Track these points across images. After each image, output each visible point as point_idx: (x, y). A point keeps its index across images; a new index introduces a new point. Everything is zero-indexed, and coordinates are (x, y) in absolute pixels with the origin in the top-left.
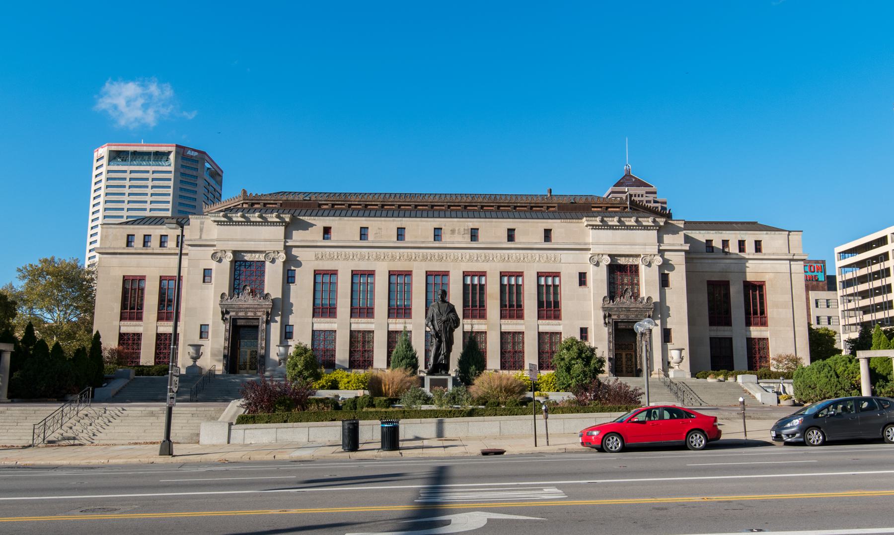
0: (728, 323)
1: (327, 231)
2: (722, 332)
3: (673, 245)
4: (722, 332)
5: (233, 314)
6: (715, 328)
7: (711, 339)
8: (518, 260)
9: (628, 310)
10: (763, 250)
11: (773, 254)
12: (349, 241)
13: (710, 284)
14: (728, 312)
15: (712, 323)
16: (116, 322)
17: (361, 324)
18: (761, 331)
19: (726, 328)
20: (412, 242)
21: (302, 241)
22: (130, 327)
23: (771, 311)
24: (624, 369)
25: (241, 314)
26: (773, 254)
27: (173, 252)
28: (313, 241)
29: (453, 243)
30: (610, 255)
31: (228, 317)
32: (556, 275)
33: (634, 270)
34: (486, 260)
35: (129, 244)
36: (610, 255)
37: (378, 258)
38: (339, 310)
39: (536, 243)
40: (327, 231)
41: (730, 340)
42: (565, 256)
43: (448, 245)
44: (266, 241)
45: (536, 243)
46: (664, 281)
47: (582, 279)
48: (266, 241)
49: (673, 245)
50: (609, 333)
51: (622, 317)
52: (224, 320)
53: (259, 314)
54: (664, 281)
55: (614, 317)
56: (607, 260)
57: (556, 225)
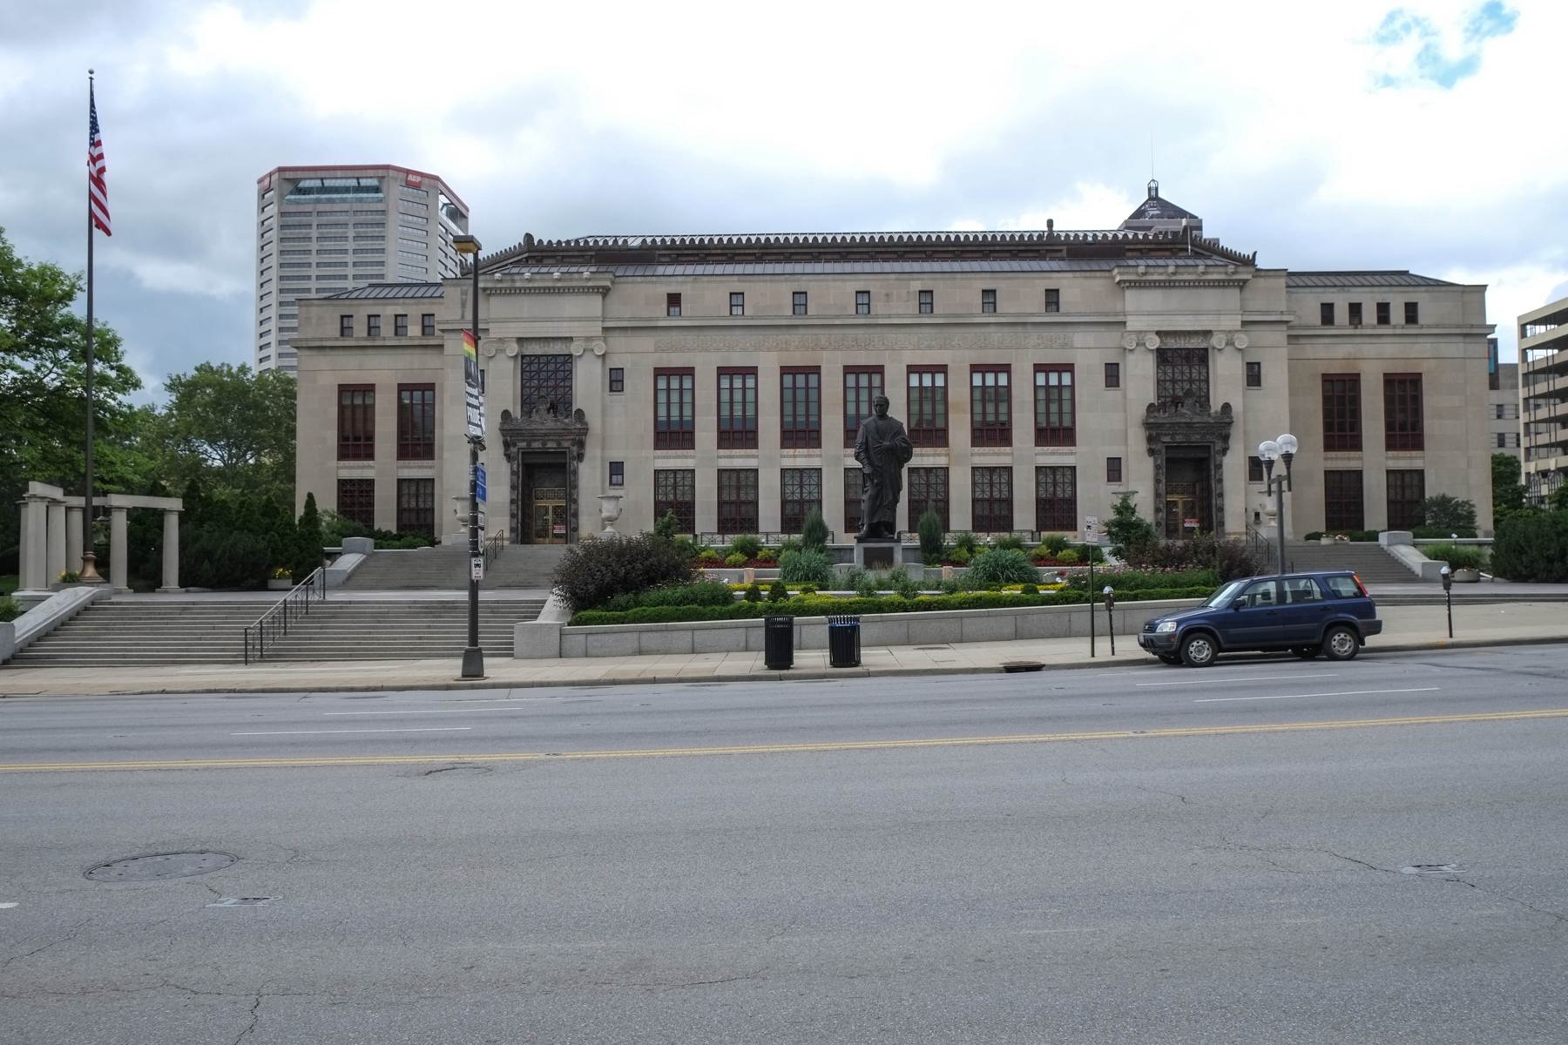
0: (1357, 446)
1: (674, 300)
2: (1343, 461)
3: (1267, 313)
5: (524, 444)
6: (1333, 454)
7: (1326, 473)
9: (1189, 425)
10: (1422, 319)
11: (1437, 326)
12: (711, 318)
13: (1328, 379)
14: (1356, 425)
15: (1329, 446)
16: (333, 462)
17: (738, 459)
20: (818, 317)
21: (629, 320)
22: (355, 470)
23: (1430, 425)
25: (536, 445)
27: (416, 342)
28: (650, 319)
29: (889, 316)
30: (1158, 333)
31: (514, 450)
32: (1069, 368)
35: (345, 330)
36: (1158, 333)
37: (757, 349)
38: (699, 436)
39: (1032, 315)
40: (674, 300)
41: (1359, 474)
42: (1080, 338)
43: (880, 321)
44: (572, 320)
45: (1032, 315)
46: (1254, 376)
47: (1112, 375)
48: (572, 320)
49: (1267, 313)
50: (1157, 467)
51: (1179, 438)
52: (508, 457)
53: (566, 444)
54: (1254, 376)
55: (1167, 439)
57: (1065, 282)
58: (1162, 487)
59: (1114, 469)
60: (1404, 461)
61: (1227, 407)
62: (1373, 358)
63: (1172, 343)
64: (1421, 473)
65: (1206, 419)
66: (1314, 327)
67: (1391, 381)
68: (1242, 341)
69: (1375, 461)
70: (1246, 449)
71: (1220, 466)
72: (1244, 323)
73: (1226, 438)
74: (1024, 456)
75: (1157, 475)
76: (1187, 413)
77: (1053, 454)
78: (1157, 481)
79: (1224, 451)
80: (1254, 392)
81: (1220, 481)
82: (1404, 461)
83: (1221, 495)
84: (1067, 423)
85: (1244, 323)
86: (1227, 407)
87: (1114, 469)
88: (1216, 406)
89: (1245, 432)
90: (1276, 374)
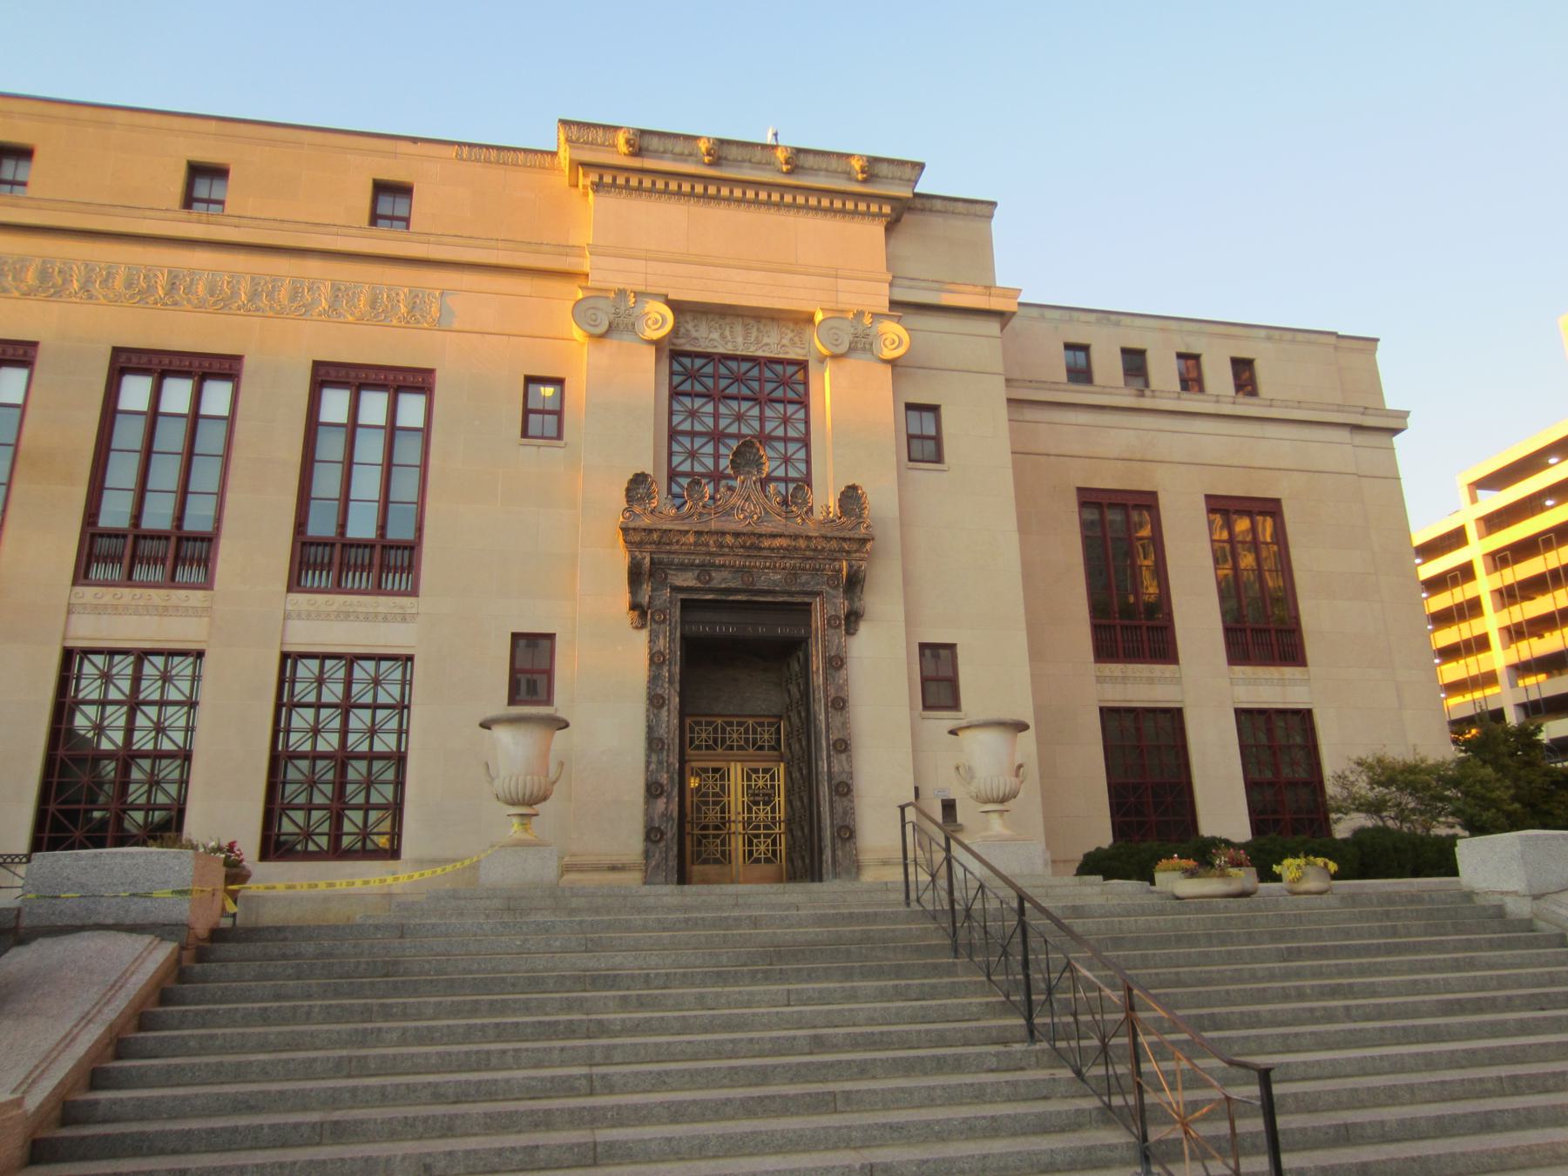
2: (1141, 686)
4: (1141, 686)
6: (1115, 669)
8: (221, 301)
11: (1300, 404)
13: (1090, 499)
18: (1282, 682)
19: (1158, 669)
23: (1314, 614)
24: (738, 845)
26: (1300, 404)
32: (418, 381)
33: (786, 383)
34: (50, 285)
41: (1175, 716)
46: (924, 440)
50: (656, 660)
51: (720, 579)
54: (924, 440)
55: (687, 580)
56: (658, 321)
58: (669, 719)
59: (531, 668)
60: (1271, 688)
61: (851, 497)
62: (1183, 462)
63: (712, 339)
64: (1305, 716)
65: (796, 526)
66: (1054, 385)
67: (1221, 507)
68: (894, 337)
69: (1208, 691)
70: (910, 622)
71: (836, 663)
72: (894, 304)
73: (854, 583)
74: (245, 620)
75: (654, 680)
76: (747, 508)
77: (345, 615)
78: (655, 701)
79: (853, 619)
80: (925, 476)
81: (839, 704)
82: (1271, 688)
83: (843, 746)
84: (399, 530)
85: (894, 304)
86: (851, 497)
87: (531, 668)
88: (825, 498)
89: (907, 582)
90: (977, 429)
